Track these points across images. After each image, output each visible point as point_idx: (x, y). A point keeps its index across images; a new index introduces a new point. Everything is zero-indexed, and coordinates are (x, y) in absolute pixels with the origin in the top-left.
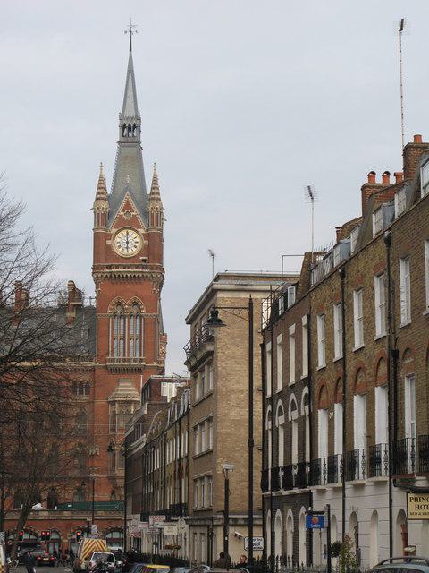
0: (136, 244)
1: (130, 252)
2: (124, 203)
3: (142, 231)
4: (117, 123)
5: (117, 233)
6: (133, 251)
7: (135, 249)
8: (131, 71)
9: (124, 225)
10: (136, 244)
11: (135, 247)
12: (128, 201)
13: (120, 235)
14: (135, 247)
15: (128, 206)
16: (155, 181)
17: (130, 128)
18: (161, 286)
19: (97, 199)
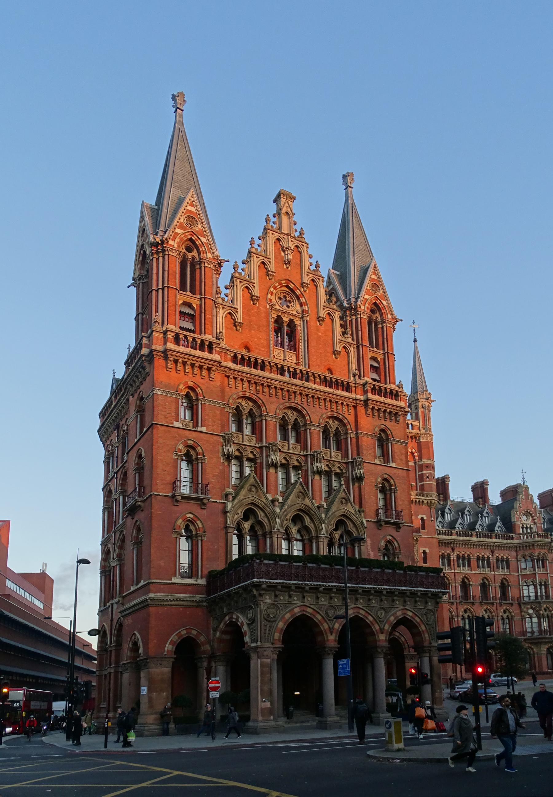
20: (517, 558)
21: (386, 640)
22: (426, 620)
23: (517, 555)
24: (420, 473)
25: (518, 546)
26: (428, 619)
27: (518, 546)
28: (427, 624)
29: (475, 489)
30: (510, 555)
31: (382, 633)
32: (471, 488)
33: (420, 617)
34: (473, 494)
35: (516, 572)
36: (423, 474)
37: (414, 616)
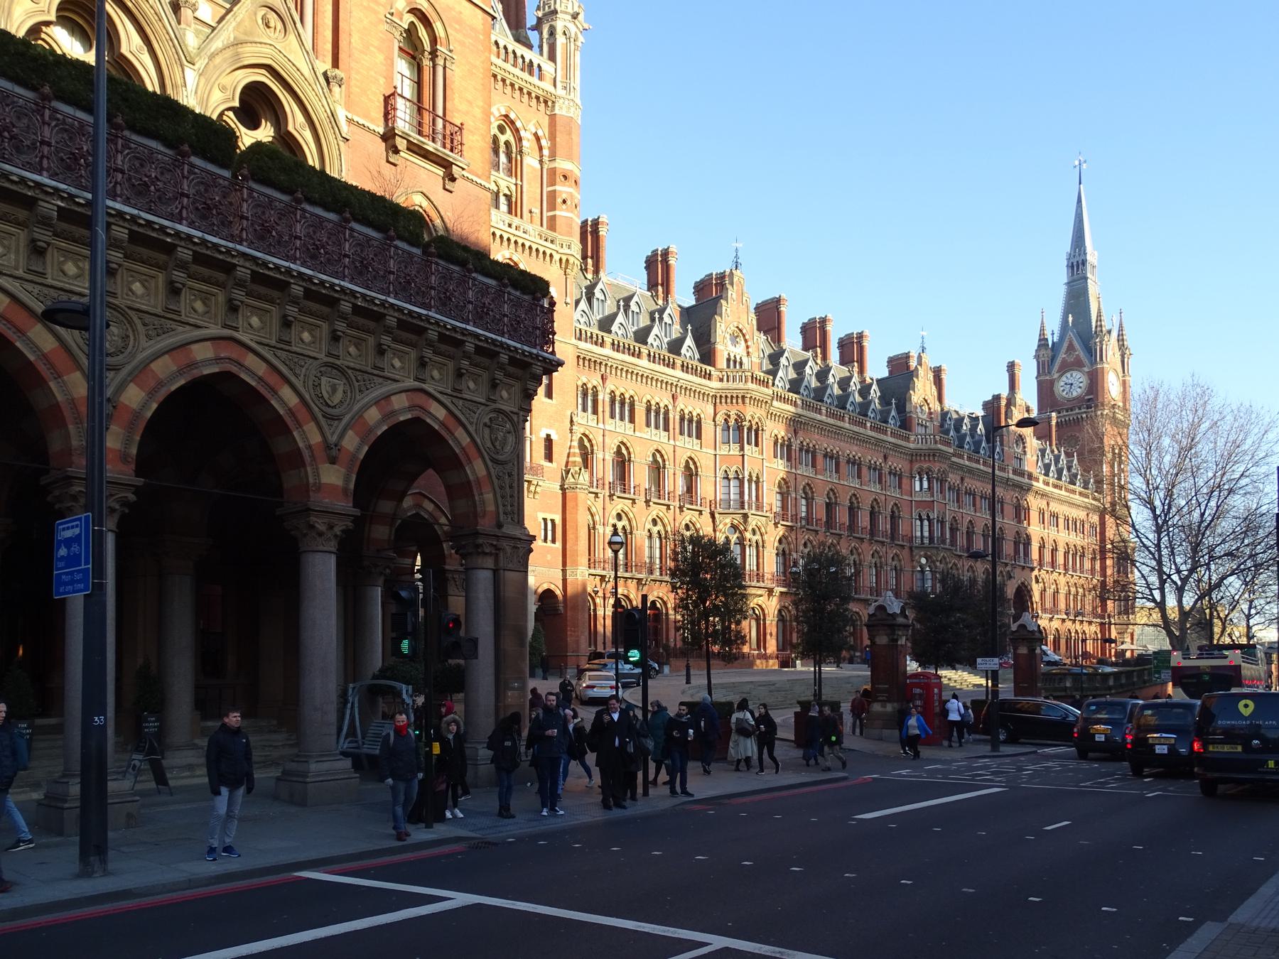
0: (1081, 385)
1: (1075, 394)
2: (1066, 345)
3: (1086, 369)
5: (1061, 376)
6: (1076, 392)
7: (1079, 390)
9: (1065, 368)
10: (1081, 385)
11: (1080, 387)
13: (1064, 378)
14: (1080, 387)
15: (1071, 348)
16: (1099, 315)
19: (1039, 346)
20: (714, 421)
21: (345, 490)
22: (489, 444)
23: (715, 415)
24: (551, 189)
25: (718, 395)
26: (497, 444)
27: (718, 395)
28: (493, 460)
29: (651, 263)
30: (704, 410)
31: (333, 461)
32: (646, 262)
33: (471, 429)
34: (648, 274)
36: (555, 191)
37: (451, 423)
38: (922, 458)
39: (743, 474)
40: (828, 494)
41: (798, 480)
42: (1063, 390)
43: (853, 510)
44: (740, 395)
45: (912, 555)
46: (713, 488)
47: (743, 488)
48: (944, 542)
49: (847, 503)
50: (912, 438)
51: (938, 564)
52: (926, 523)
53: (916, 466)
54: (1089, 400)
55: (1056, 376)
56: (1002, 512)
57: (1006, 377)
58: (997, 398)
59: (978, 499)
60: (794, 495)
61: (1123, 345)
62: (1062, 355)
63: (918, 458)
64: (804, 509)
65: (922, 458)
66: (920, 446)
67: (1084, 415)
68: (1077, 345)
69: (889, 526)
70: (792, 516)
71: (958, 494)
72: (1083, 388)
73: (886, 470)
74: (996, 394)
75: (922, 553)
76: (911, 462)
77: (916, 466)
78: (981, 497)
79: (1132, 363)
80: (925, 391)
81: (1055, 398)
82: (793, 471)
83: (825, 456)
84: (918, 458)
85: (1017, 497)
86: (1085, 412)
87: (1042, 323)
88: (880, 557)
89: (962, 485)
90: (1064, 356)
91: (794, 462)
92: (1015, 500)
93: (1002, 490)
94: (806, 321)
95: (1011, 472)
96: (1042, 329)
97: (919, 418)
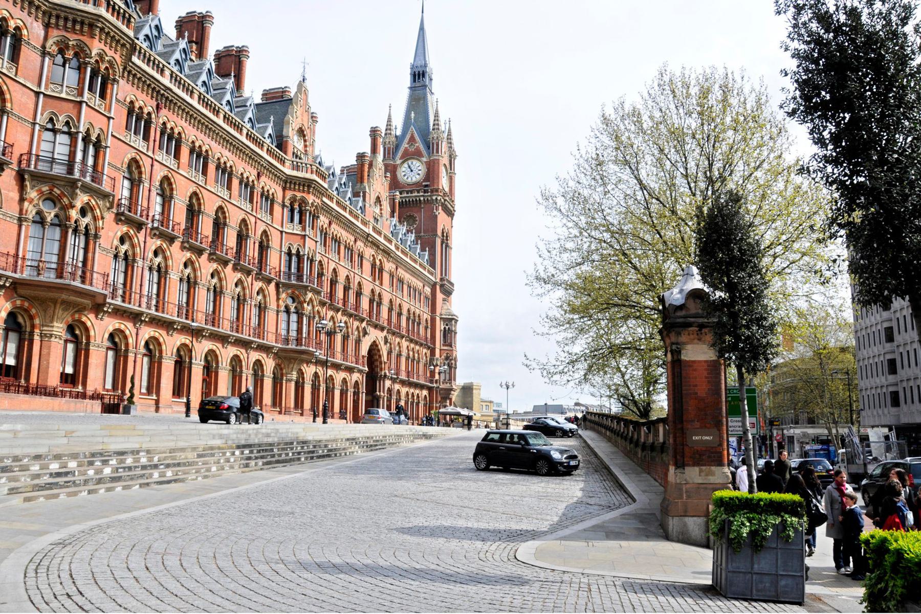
0: (420, 172)
2: (408, 137)
3: (424, 159)
4: (408, 71)
5: (403, 162)
7: (418, 176)
8: (422, 29)
9: (407, 156)
10: (420, 172)
11: (419, 174)
12: (412, 134)
13: (406, 165)
14: (419, 174)
15: (412, 139)
17: (419, 76)
18: (450, 213)
23: (46, 38)
25: (54, 13)
35: (32, 83)
38: (297, 188)
39: (77, 127)
40: (191, 198)
41: (155, 167)
42: (405, 175)
43: (219, 225)
44: (87, 21)
45: (278, 294)
46: (28, 139)
47: (75, 146)
48: (311, 281)
49: (213, 214)
50: (288, 163)
51: (305, 305)
52: (294, 259)
53: (289, 194)
54: (426, 186)
55: (399, 162)
56: (362, 267)
57: (369, 141)
58: (361, 157)
59: (342, 247)
60: (147, 185)
61: (451, 147)
62: (405, 145)
63: (292, 186)
64: (158, 209)
65: (297, 188)
66: (294, 173)
67: (422, 199)
68: (417, 138)
69: (256, 255)
70: (142, 211)
71: (325, 238)
72: (421, 176)
73: (258, 191)
74: (361, 152)
75: (290, 291)
76: (284, 189)
77: (289, 194)
78: (345, 247)
79: (458, 163)
80: (302, 120)
81: (398, 182)
82: (150, 154)
83: (192, 151)
84: (292, 186)
85: (373, 255)
86: (423, 196)
87: (390, 115)
88: (244, 289)
89: (330, 230)
90: (406, 146)
91: (151, 143)
92: (372, 258)
93: (362, 245)
94: (184, 15)
95: (371, 227)
96: (389, 120)
97: (294, 147)
